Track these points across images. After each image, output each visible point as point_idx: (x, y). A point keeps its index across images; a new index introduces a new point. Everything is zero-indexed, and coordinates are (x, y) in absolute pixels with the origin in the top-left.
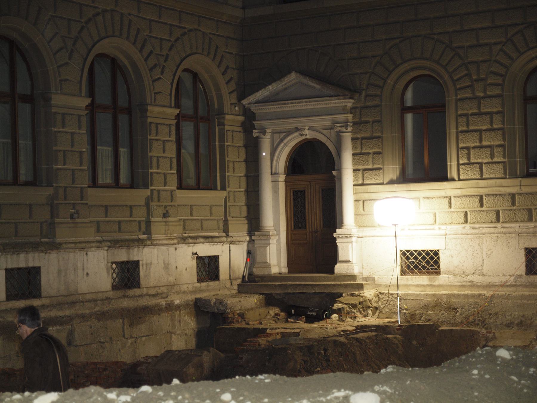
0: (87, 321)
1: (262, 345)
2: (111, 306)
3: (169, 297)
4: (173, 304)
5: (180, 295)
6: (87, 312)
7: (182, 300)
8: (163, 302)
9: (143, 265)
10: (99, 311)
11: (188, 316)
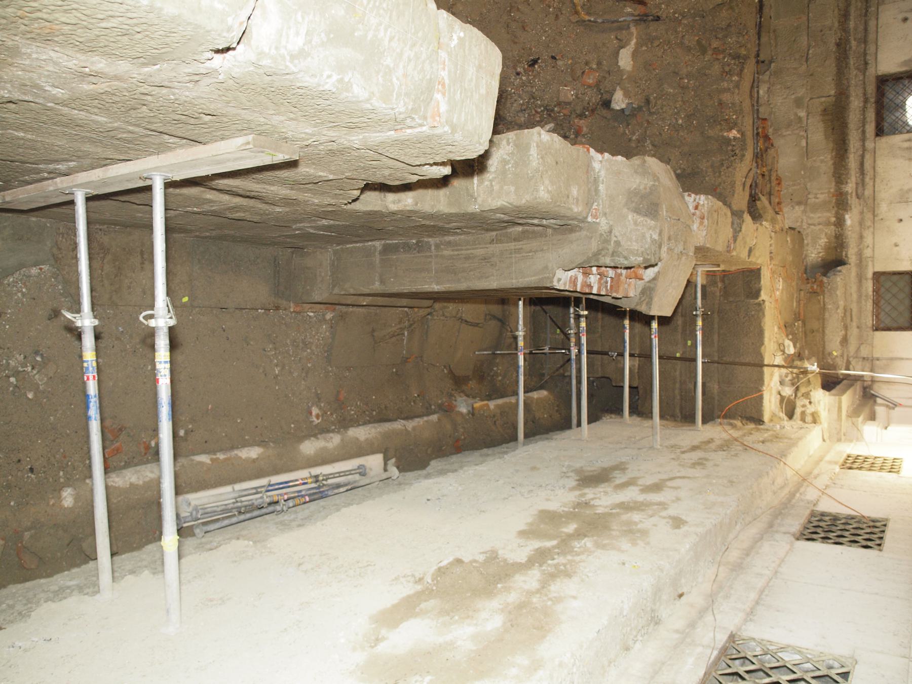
1: (767, 155)
2: (855, 72)
3: (857, 200)
4: (846, 210)
5: (857, 228)
7: (850, 233)
8: (850, 187)
11: (826, 242)
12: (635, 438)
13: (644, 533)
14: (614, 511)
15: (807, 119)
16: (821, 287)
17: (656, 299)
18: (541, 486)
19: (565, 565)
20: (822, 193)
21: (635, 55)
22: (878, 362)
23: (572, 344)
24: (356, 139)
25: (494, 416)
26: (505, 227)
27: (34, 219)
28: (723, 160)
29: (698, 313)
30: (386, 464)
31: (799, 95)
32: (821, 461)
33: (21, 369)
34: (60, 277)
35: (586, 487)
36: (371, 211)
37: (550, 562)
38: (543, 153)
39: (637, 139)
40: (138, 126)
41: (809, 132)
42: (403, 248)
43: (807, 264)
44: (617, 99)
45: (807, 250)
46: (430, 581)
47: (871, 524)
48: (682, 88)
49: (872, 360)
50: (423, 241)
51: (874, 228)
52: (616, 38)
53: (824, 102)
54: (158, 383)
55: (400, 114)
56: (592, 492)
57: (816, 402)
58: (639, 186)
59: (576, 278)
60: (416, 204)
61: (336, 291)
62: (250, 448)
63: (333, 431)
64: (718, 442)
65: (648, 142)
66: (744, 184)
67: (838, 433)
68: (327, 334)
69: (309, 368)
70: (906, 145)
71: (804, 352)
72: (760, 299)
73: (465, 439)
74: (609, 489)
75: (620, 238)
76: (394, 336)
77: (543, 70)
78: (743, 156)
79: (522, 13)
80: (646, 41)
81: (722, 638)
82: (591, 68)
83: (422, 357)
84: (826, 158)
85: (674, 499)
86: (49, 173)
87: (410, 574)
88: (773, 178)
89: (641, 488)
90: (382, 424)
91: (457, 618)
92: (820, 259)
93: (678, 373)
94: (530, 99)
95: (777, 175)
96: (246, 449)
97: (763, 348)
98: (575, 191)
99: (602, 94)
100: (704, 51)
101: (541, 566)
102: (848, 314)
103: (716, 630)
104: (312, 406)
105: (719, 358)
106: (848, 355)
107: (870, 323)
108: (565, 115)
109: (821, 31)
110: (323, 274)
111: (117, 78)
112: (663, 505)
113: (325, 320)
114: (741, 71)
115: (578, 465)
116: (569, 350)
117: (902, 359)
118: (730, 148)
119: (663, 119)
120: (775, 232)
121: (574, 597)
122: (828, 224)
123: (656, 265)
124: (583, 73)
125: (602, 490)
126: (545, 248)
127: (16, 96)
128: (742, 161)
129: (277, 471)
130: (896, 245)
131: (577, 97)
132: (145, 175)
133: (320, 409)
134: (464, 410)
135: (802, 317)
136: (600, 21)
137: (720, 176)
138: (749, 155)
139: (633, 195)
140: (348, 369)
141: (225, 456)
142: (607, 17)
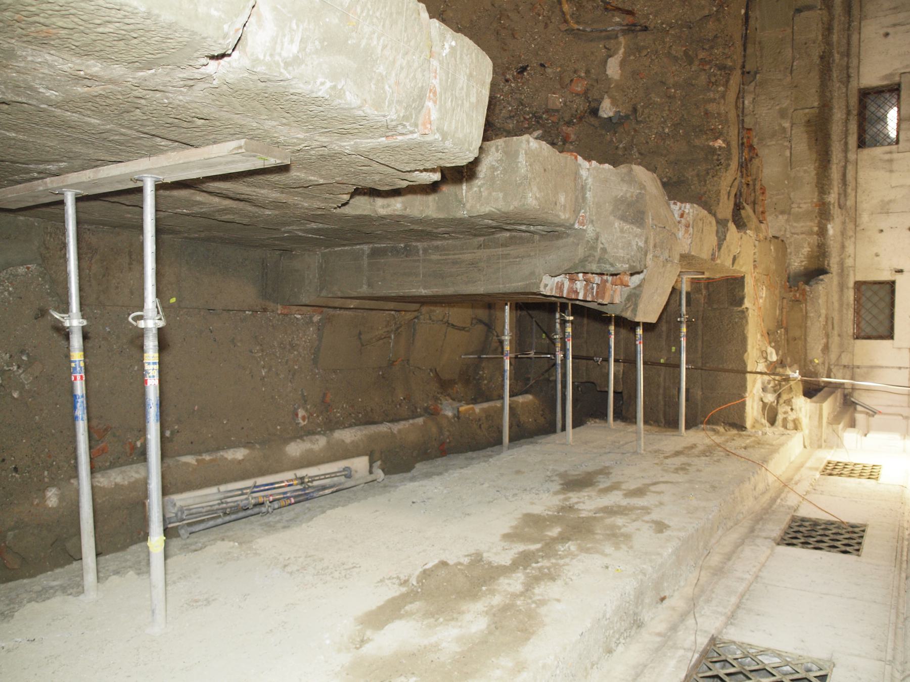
0: (823, 35)
2: (838, 85)
3: (839, 210)
4: (828, 220)
5: (839, 238)
6: (835, 38)
8: (832, 198)
9: (891, 152)
10: (833, 61)
12: (619, 442)
13: (628, 537)
14: (597, 515)
15: (791, 130)
16: (804, 295)
17: (641, 306)
18: (526, 490)
19: (549, 568)
20: (805, 203)
21: (623, 64)
22: (858, 370)
23: (558, 349)
24: (347, 145)
25: (480, 420)
26: (493, 233)
27: (21, 218)
28: (708, 169)
29: (683, 319)
30: (371, 466)
31: (784, 106)
32: (802, 467)
33: (6, 368)
34: (47, 277)
35: (570, 491)
36: (360, 215)
37: (534, 565)
38: (532, 160)
39: (624, 147)
40: (131, 128)
41: (793, 142)
42: (391, 252)
43: (790, 273)
44: (605, 107)
45: (790, 259)
46: (415, 583)
47: (850, 529)
48: (669, 97)
49: (853, 368)
50: (411, 245)
51: (855, 238)
52: (605, 48)
53: (808, 113)
54: (146, 383)
55: (392, 121)
56: (576, 496)
57: (798, 409)
58: (626, 194)
59: (563, 284)
60: (405, 209)
61: (324, 293)
62: (235, 449)
63: (319, 433)
64: (701, 448)
65: (635, 150)
66: (729, 193)
67: (819, 440)
68: (314, 336)
69: (295, 370)
70: (887, 157)
71: (786, 359)
72: (744, 307)
73: (450, 442)
74: (593, 494)
75: (606, 246)
76: (380, 339)
77: (532, 77)
78: (729, 165)
79: (512, 20)
80: (635, 50)
81: (703, 641)
82: (580, 77)
83: (408, 360)
84: (809, 168)
85: (657, 503)
86: (39, 173)
87: (395, 576)
88: (758, 187)
89: (625, 492)
90: (367, 426)
91: (441, 620)
92: (803, 268)
93: (662, 379)
94: (518, 106)
95: (761, 185)
96: (232, 450)
97: (746, 355)
98: (562, 199)
99: (590, 102)
100: (691, 63)
101: (525, 568)
102: (830, 323)
103: (698, 633)
104: (298, 408)
105: (702, 363)
106: (829, 363)
107: (851, 331)
108: (553, 122)
109: (806, 44)
110: (311, 276)
111: (111, 81)
112: (646, 510)
113: (312, 322)
114: (727, 81)
115: (562, 469)
116: (555, 355)
117: (882, 367)
118: (716, 157)
119: (650, 128)
120: (759, 241)
121: (558, 601)
122: (811, 233)
123: (642, 272)
124: (572, 81)
125: (586, 494)
126: (532, 254)
127: (10, 96)
128: (727, 170)
129: (263, 473)
130: (877, 255)
131: (565, 104)
132: (136, 177)
133: (307, 410)
134: (450, 414)
135: (784, 325)
136: (588, 29)
137: (705, 185)
138: (734, 165)
139: (619, 202)
140: (335, 371)
141: (211, 458)
142: (595, 26)
